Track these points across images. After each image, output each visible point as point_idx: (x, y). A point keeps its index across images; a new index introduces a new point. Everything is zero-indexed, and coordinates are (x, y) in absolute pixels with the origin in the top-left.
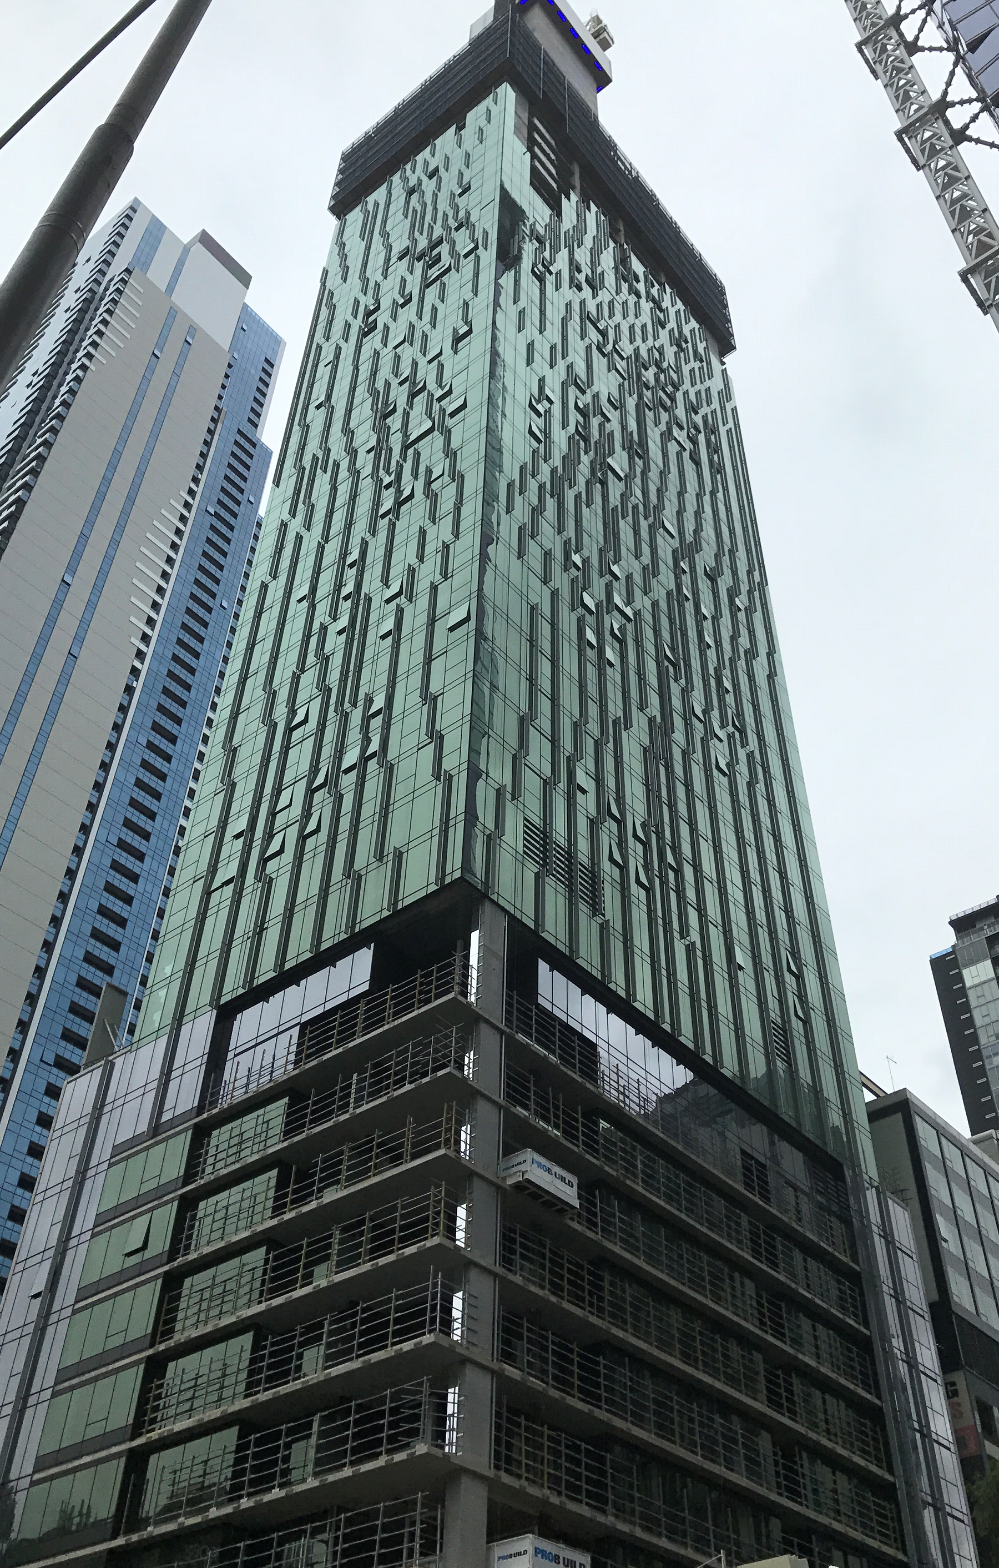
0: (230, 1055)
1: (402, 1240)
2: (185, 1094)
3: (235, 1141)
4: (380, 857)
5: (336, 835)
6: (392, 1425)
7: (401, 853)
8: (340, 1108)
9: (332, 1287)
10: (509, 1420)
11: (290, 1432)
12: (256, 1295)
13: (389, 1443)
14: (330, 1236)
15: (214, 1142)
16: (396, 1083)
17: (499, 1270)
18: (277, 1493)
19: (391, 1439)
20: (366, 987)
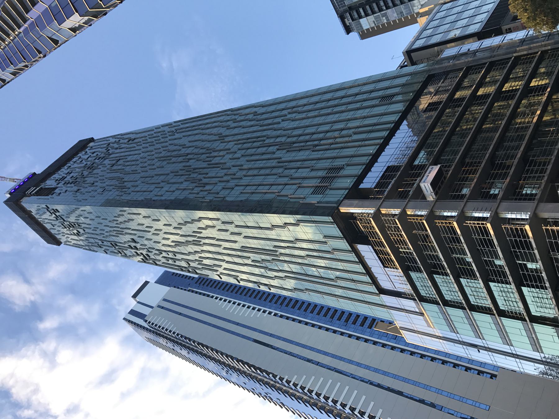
0: (395, 290)
1: (455, 234)
2: (410, 304)
3: (424, 288)
4: (325, 243)
5: (320, 257)
6: (519, 237)
7: (325, 236)
8: (411, 255)
9: (472, 257)
10: (518, 196)
11: (523, 270)
12: (476, 281)
13: (525, 238)
14: (455, 258)
15: (425, 295)
16: (402, 237)
17: (465, 200)
18: (544, 274)
19: (524, 237)
20: (370, 247)
